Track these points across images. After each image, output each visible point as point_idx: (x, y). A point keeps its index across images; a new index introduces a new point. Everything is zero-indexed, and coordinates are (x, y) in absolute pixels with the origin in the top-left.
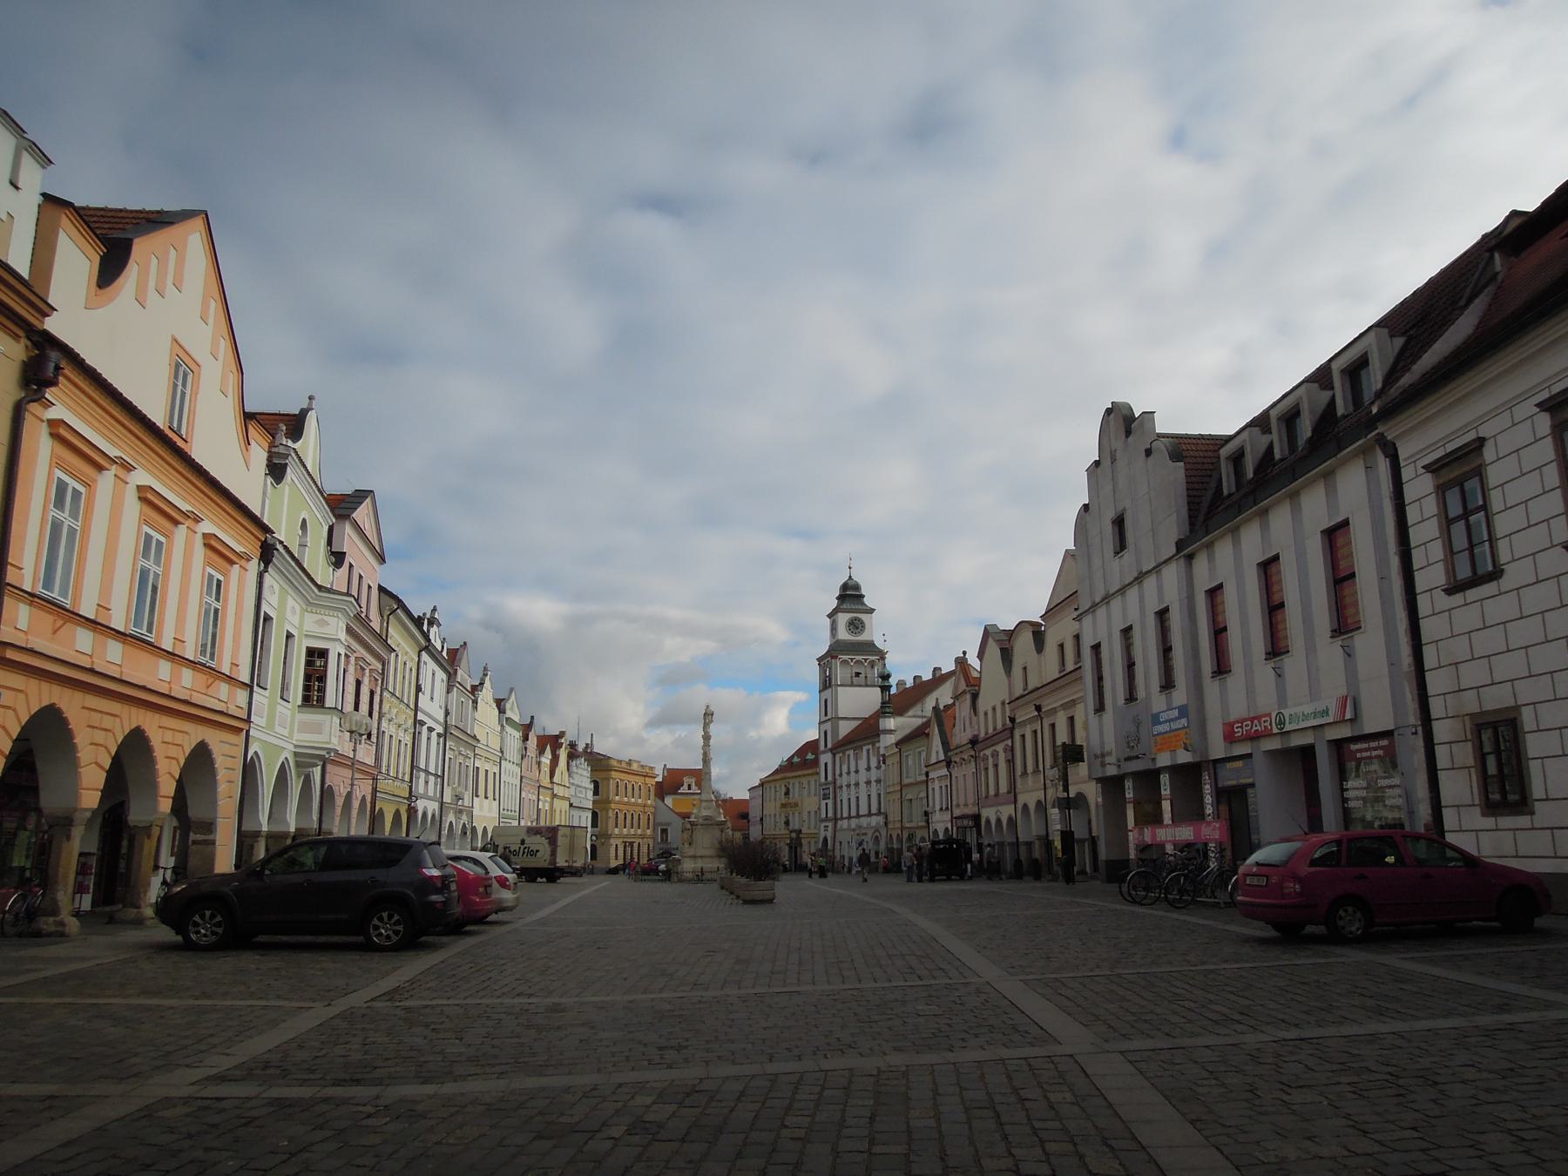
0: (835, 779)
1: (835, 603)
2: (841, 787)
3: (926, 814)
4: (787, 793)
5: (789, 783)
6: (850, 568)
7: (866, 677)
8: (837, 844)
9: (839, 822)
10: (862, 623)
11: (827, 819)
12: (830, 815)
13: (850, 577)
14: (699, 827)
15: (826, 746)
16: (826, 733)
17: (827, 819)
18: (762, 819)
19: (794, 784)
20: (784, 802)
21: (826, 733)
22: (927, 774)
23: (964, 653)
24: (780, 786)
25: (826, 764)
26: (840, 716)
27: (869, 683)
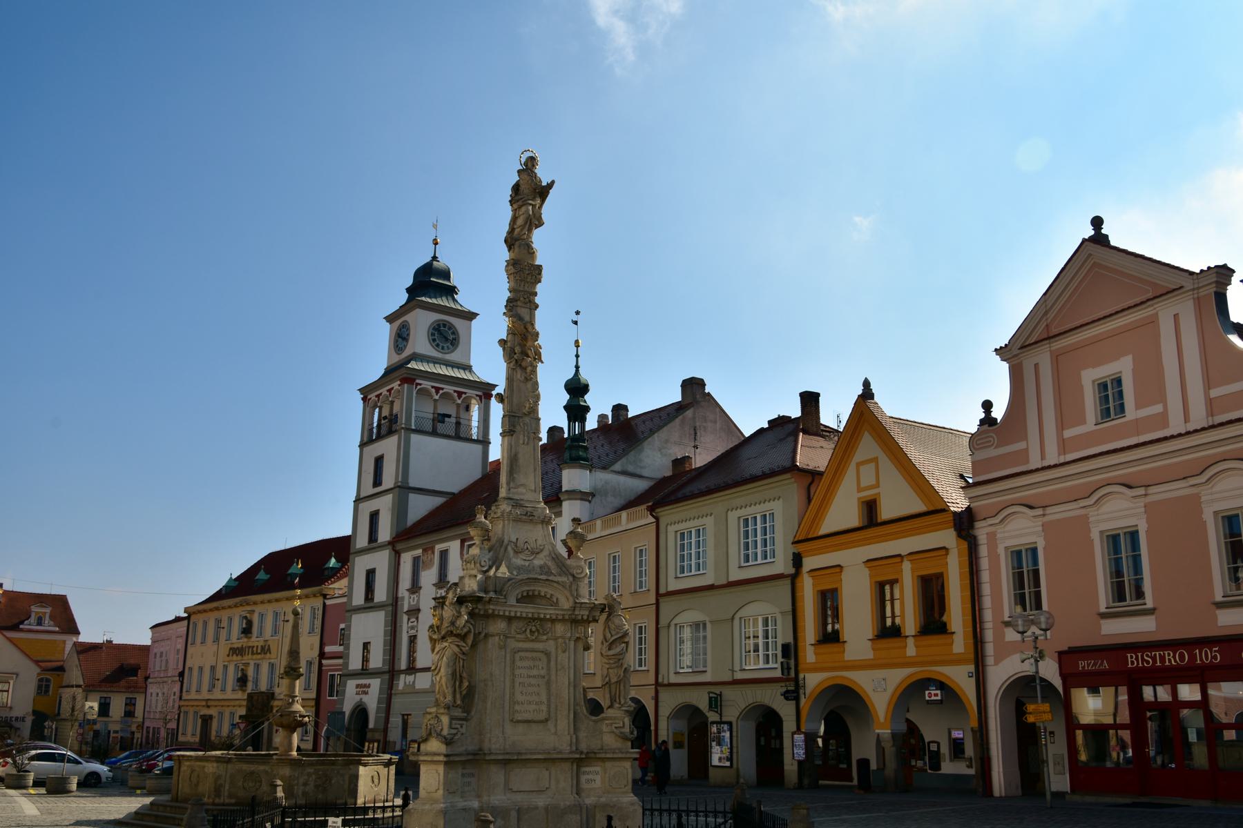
0: (395, 601)
1: (403, 297)
2: (415, 612)
3: (790, 651)
4: (247, 631)
5: (252, 612)
6: (436, 244)
7: (458, 424)
8: (396, 721)
9: (403, 681)
10: (455, 333)
11: (365, 672)
12: (377, 661)
13: (435, 258)
14: (501, 626)
15: (373, 536)
16: (374, 516)
17: (365, 672)
18: (181, 674)
19: (262, 616)
20: (235, 646)
21: (374, 516)
22: (797, 560)
23: (1097, 222)
24: (230, 619)
25: (371, 574)
26: (412, 484)
27: (462, 436)
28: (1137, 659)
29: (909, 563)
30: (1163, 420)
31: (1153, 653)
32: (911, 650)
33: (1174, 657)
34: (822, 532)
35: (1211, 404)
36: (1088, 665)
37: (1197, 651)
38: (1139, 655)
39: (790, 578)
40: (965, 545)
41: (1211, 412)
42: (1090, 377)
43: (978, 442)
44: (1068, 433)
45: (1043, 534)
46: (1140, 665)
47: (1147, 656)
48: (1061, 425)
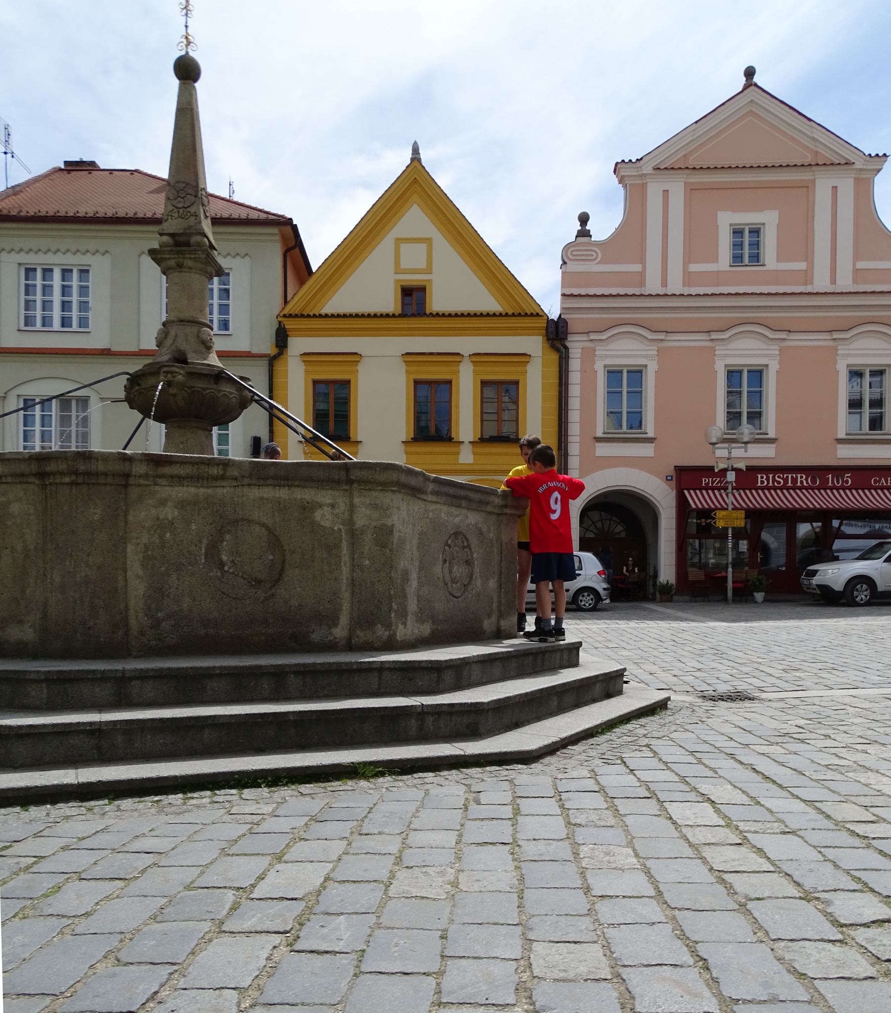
22: (282, 338)
28: (768, 479)
29: (471, 365)
30: (807, 276)
31: (785, 475)
32: (466, 456)
33: (807, 480)
34: (327, 310)
35: (858, 274)
36: (713, 483)
37: (830, 476)
38: (771, 476)
39: (267, 359)
40: (554, 357)
41: (855, 281)
42: (726, 220)
43: (574, 253)
44: (694, 268)
45: (657, 359)
46: (771, 484)
47: (779, 477)
48: (688, 258)
